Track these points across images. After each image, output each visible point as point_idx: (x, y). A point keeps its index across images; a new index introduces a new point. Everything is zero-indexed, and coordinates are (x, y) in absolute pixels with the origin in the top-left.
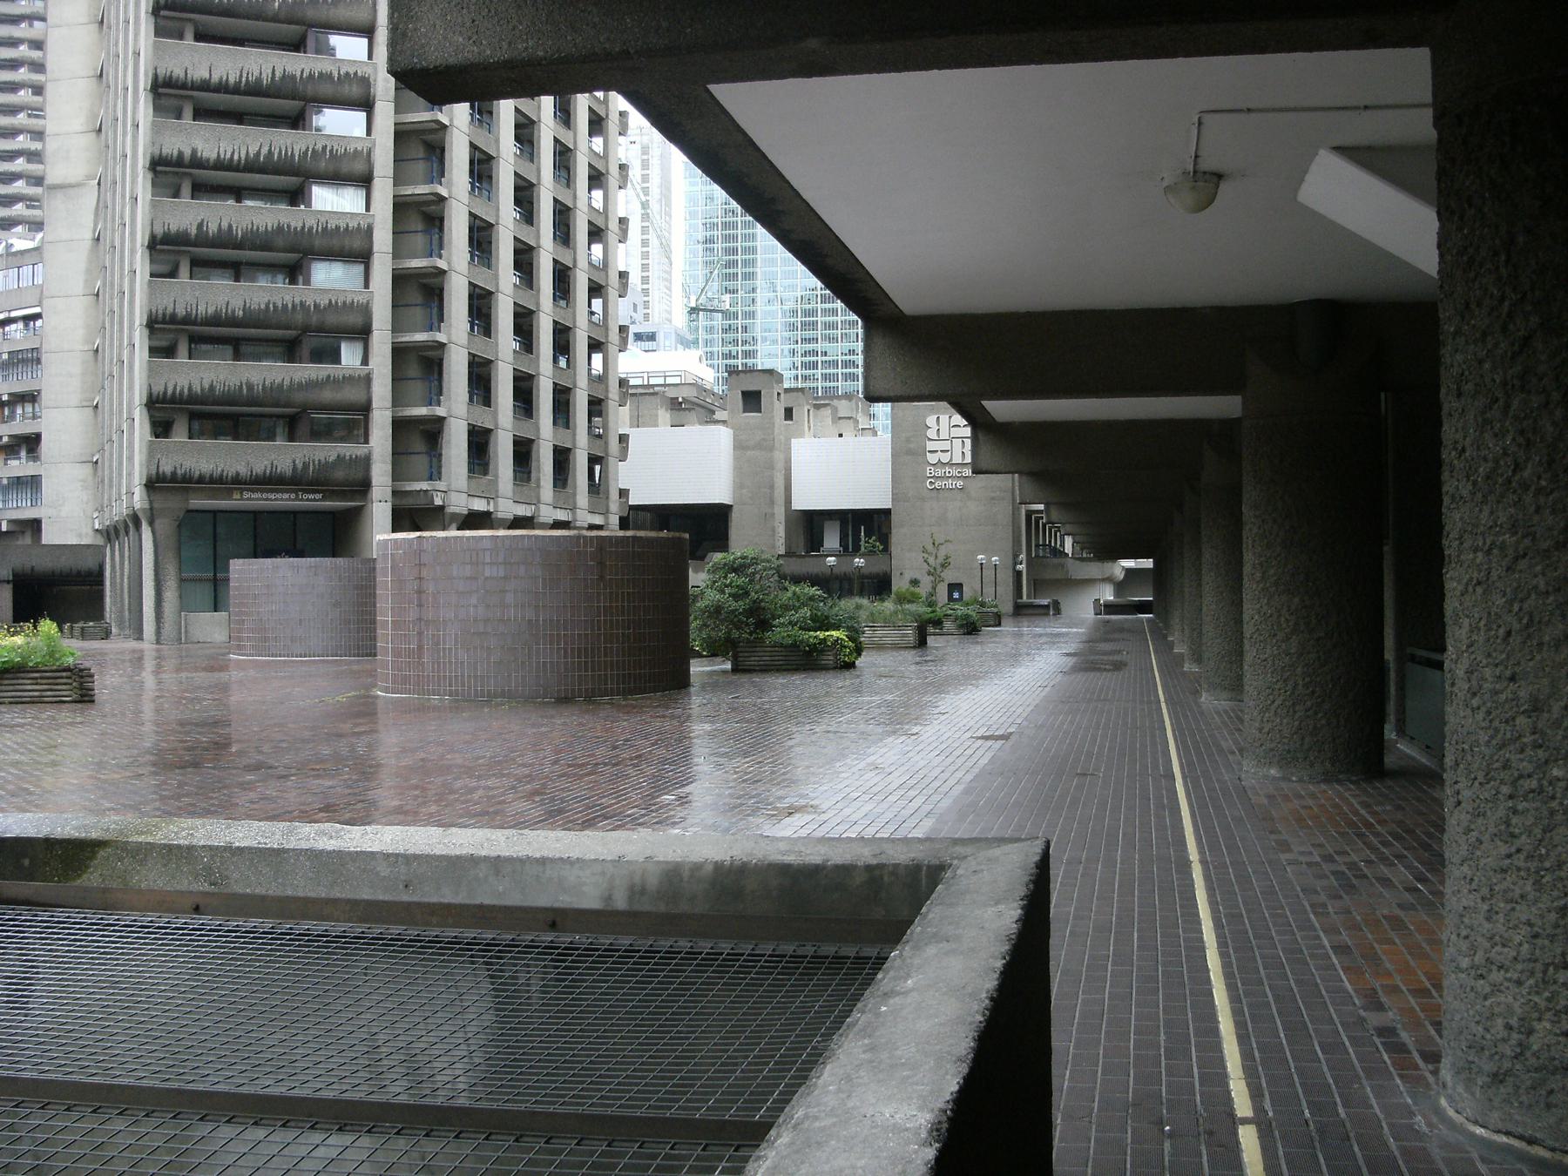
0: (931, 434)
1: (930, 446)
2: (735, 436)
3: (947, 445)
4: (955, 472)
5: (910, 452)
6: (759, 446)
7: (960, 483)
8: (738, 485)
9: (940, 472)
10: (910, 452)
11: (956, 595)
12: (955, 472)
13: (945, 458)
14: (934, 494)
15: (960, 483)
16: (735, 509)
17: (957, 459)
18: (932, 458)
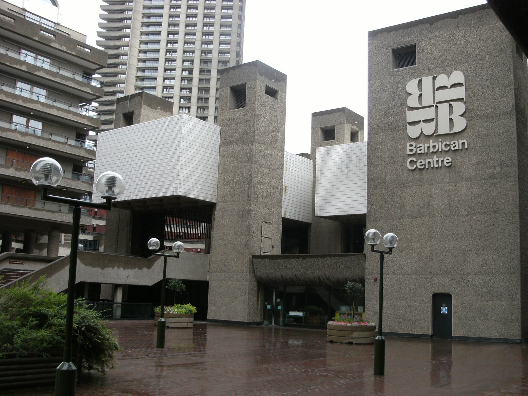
0: (412, 102)
1: (411, 116)
2: (222, 132)
3: (430, 113)
4: (440, 145)
5: (388, 128)
6: (241, 140)
7: (447, 160)
8: (223, 182)
9: (423, 147)
10: (388, 128)
11: (444, 310)
12: (440, 145)
13: (429, 129)
14: (416, 176)
15: (447, 160)
16: (218, 207)
17: (444, 129)
18: (413, 132)
